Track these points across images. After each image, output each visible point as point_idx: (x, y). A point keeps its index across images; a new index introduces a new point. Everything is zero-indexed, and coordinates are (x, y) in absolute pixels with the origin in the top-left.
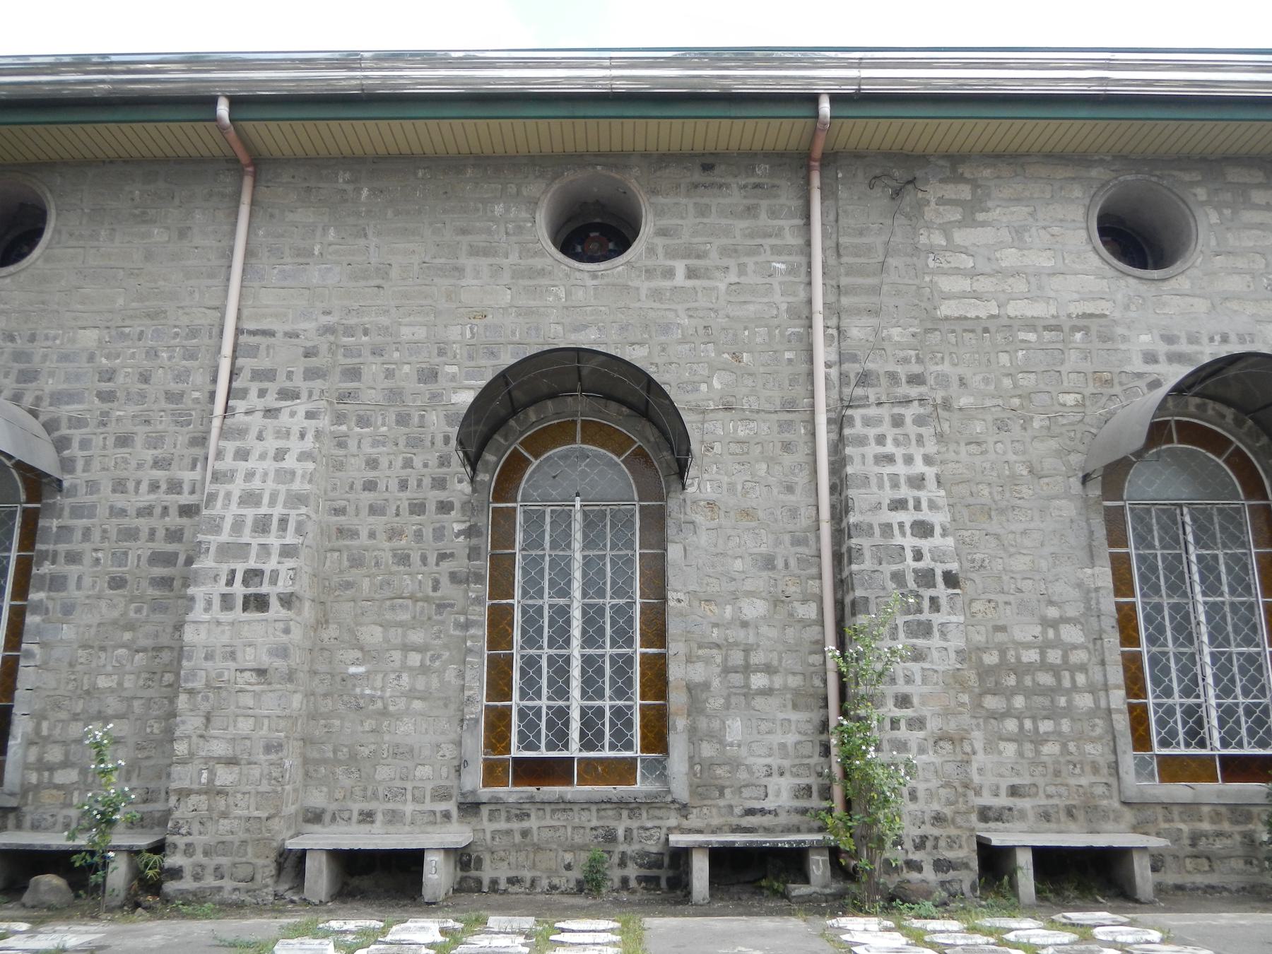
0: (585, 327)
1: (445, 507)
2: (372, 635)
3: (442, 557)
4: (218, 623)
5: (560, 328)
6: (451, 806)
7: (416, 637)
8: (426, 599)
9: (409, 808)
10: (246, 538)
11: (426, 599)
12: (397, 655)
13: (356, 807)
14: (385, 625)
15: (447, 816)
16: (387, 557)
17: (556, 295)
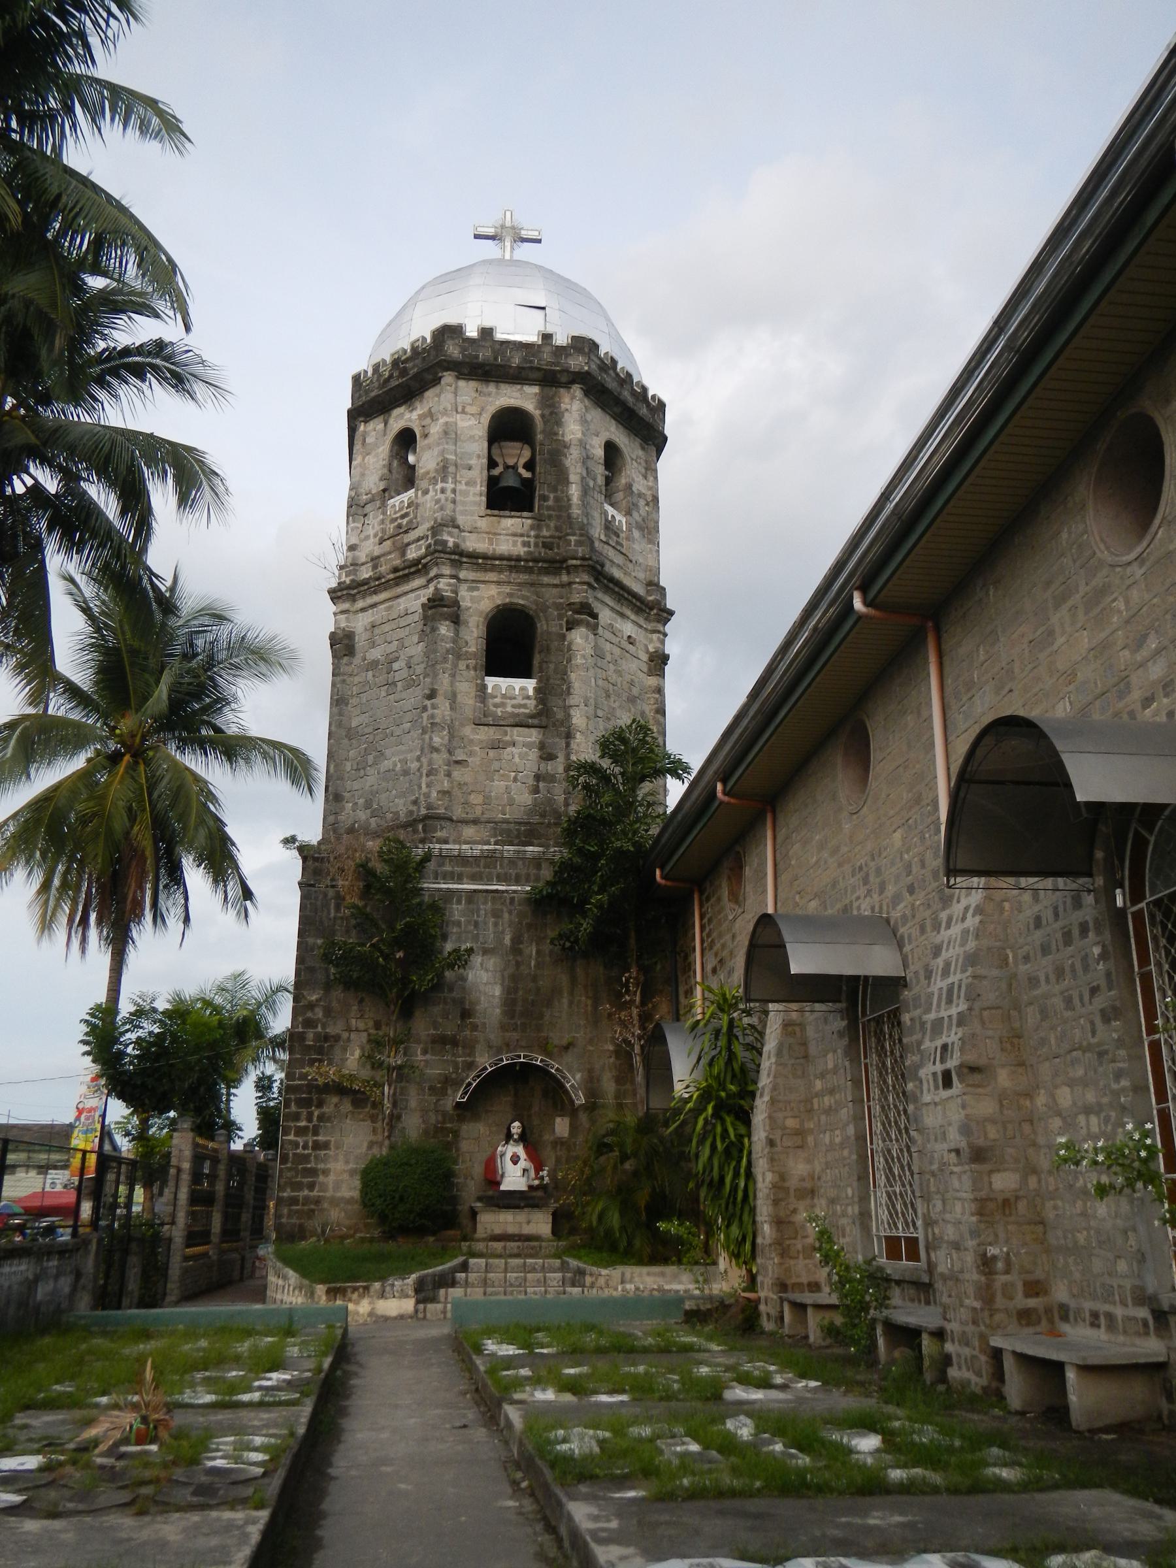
0: (1145, 637)
1: (1084, 929)
2: (1065, 1097)
3: (1094, 991)
4: (936, 1104)
5: (1126, 653)
6: (1143, 1313)
7: (1090, 1097)
8: (1088, 1048)
9: (1119, 1312)
10: (944, 1014)
11: (1088, 1048)
12: (1081, 1119)
13: (1088, 1305)
14: (1071, 1083)
15: (1145, 1324)
16: (1058, 1002)
17: (1119, 612)
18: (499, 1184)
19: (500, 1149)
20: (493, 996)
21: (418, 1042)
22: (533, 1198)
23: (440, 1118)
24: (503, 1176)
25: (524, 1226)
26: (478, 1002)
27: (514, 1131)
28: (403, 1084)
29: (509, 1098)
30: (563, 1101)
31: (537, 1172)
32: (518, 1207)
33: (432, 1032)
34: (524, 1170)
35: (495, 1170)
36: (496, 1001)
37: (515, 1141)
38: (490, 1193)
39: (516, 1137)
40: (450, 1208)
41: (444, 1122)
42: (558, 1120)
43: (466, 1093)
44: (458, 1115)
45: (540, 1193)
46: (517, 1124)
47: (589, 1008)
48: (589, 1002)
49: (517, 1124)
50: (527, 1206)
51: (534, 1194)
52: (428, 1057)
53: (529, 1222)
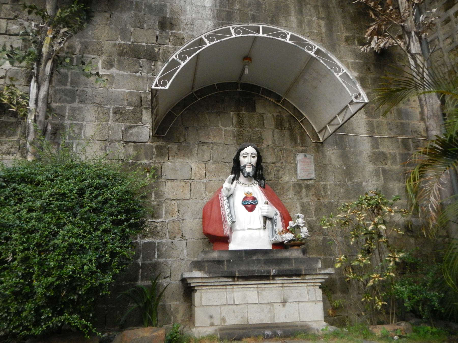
18: (226, 240)
19: (226, 185)
20: (204, 7)
21: (100, 53)
22: (287, 260)
23: (131, 150)
24: (231, 229)
25: (278, 307)
26: (184, 12)
27: (244, 161)
28: (75, 105)
29: (230, 128)
30: (303, 133)
31: (286, 224)
32: (266, 277)
33: (119, 41)
34: (266, 218)
35: (220, 221)
36: (208, 13)
37: (248, 176)
38: (215, 255)
39: (249, 170)
40: (149, 283)
41: (137, 158)
42: (300, 157)
43: (168, 77)
44: (157, 148)
45: (295, 253)
46: (250, 150)
47: (323, 30)
48: (322, 23)
49: (250, 150)
50: (280, 274)
51: (286, 254)
52: (114, 71)
53: (284, 302)
